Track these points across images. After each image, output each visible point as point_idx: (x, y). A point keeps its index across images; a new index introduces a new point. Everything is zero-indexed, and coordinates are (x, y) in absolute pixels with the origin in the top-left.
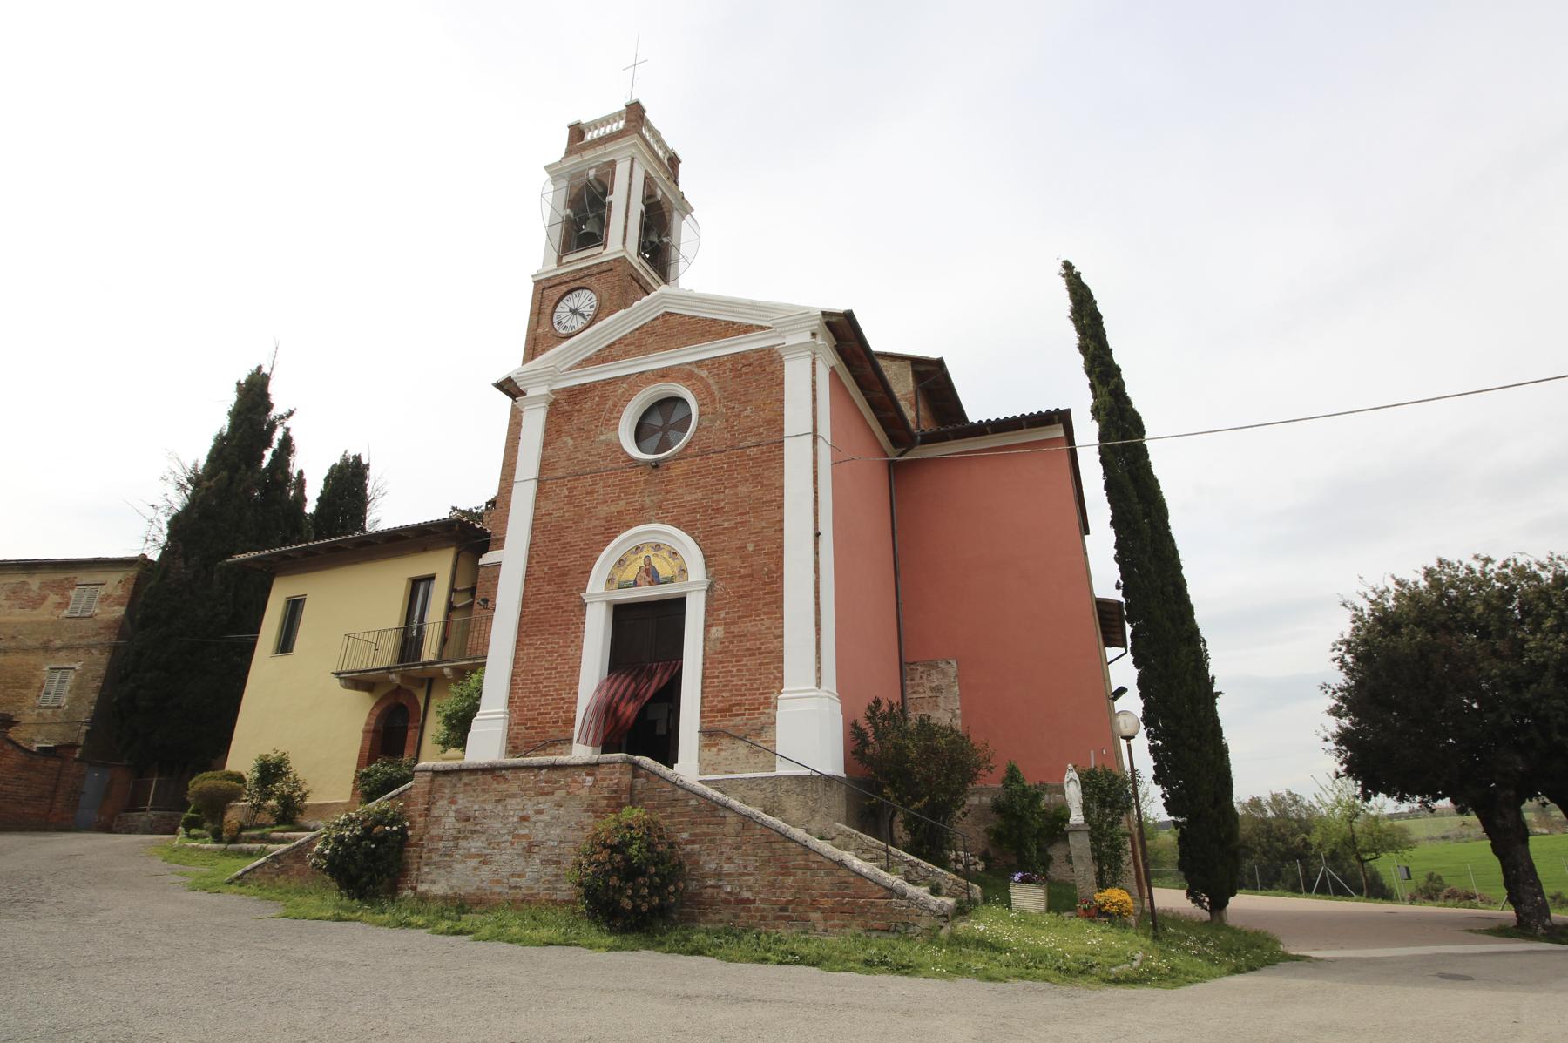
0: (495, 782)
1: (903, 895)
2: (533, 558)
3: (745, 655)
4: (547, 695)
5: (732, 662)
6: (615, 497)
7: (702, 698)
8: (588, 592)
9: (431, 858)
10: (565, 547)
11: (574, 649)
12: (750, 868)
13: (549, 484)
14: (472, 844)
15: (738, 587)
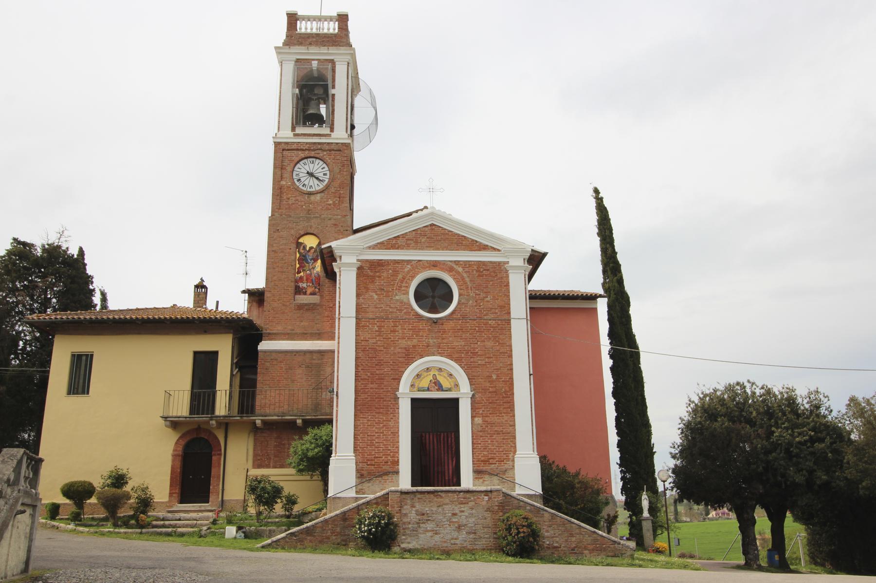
0: (435, 498)
1: (619, 544)
2: (358, 366)
3: (494, 434)
4: (379, 447)
5: (487, 437)
6: (410, 336)
7: (473, 454)
8: (400, 392)
9: (405, 532)
10: (380, 363)
11: (393, 422)
12: (557, 535)
13: (364, 321)
14: (428, 526)
15: (489, 397)
